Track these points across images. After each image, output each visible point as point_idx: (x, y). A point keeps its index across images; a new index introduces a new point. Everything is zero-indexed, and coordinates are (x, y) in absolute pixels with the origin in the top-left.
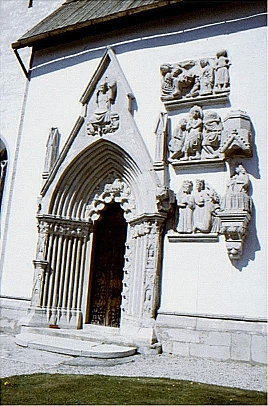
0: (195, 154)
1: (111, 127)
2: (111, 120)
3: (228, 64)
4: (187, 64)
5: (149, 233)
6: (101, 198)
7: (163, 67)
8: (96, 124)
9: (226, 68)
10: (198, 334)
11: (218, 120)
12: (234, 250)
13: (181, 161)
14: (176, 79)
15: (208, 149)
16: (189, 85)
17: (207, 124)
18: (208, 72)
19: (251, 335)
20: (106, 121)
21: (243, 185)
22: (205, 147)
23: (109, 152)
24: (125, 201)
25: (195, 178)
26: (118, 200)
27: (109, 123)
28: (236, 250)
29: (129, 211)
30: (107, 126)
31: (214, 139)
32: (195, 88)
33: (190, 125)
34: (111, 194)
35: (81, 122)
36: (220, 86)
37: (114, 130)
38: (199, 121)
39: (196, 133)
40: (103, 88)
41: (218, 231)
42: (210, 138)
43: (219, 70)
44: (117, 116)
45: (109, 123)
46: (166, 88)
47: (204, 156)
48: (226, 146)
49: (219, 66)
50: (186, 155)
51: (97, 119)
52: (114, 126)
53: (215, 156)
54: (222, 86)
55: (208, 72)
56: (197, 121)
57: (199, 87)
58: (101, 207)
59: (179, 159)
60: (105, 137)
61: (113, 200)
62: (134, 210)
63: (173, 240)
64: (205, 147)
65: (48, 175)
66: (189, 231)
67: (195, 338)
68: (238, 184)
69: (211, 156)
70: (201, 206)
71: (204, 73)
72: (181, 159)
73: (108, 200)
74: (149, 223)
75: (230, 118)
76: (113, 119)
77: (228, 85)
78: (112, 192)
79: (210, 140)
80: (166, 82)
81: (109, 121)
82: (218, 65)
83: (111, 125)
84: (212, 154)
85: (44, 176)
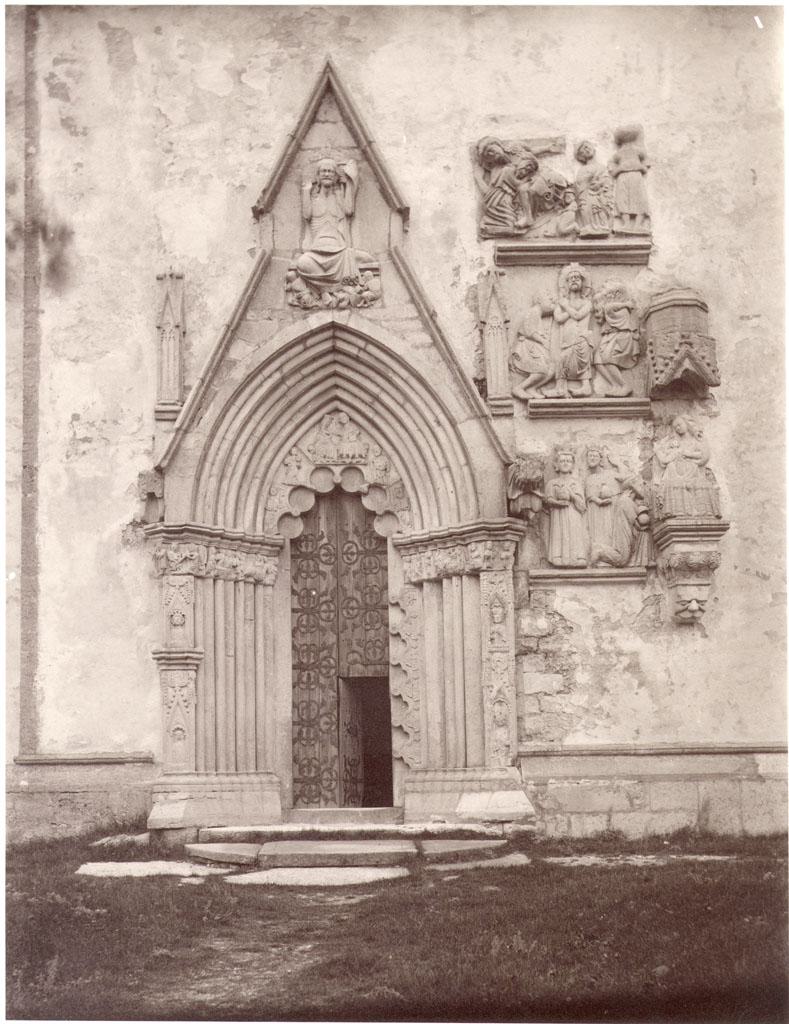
0: (577, 379)
1: (360, 292)
2: (359, 274)
4: (545, 147)
5: (489, 569)
6: (302, 478)
7: (490, 147)
9: (639, 174)
11: (629, 304)
12: (694, 602)
13: (546, 398)
14: (524, 186)
15: (610, 372)
16: (551, 200)
17: (609, 313)
18: (598, 179)
19: (740, 781)
20: (346, 274)
21: (698, 461)
22: (602, 368)
23: (340, 358)
24: (375, 486)
27: (352, 282)
28: (698, 602)
30: (346, 288)
31: (625, 350)
33: (563, 309)
34: (332, 468)
35: (265, 266)
36: (626, 218)
38: (586, 305)
39: (580, 331)
40: (327, 178)
41: (645, 563)
42: (617, 347)
43: (622, 177)
44: (375, 265)
45: (352, 282)
46: (498, 204)
47: (597, 388)
49: (622, 167)
50: (559, 383)
52: (368, 290)
53: (623, 391)
54: (633, 217)
55: (598, 179)
56: (578, 302)
60: (340, 317)
62: (407, 512)
64: (602, 368)
65: (177, 412)
66: (581, 562)
68: (687, 457)
70: (603, 505)
71: (590, 179)
72: (550, 392)
74: (489, 544)
75: (675, 306)
76: (361, 270)
77: (646, 217)
79: (620, 352)
81: (353, 277)
82: (617, 162)
83: (358, 288)
84: (621, 385)
85: (157, 412)
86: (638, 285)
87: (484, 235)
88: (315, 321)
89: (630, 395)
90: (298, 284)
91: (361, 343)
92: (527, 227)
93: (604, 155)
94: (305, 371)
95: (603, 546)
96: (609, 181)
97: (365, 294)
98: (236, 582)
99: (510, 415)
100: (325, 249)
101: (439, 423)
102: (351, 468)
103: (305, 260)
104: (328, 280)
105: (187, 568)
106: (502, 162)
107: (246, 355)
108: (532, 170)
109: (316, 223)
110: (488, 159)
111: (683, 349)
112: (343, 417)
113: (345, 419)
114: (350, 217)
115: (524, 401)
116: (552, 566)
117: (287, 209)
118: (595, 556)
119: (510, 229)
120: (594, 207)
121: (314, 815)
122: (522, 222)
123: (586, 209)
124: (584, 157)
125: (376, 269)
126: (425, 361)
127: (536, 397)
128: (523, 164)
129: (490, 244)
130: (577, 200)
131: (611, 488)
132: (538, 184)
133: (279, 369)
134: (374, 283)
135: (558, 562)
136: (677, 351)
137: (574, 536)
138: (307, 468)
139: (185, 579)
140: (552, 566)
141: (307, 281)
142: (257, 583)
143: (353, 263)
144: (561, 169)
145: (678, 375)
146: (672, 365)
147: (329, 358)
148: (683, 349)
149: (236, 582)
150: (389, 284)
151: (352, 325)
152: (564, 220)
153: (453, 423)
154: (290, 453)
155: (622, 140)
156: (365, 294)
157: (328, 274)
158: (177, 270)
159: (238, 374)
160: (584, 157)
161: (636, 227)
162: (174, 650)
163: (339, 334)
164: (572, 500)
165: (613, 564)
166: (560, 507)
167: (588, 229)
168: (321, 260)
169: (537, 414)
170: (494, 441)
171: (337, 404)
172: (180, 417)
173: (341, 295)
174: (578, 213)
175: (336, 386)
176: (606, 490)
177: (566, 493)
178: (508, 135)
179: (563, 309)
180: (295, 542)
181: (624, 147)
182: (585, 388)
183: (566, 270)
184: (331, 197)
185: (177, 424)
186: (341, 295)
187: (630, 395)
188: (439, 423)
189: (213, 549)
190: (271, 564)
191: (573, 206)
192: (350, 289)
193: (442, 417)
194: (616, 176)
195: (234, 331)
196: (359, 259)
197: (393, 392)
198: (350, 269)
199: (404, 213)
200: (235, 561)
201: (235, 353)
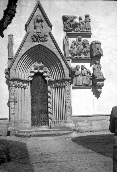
0: (80, 55)
3: (90, 21)
5: (66, 86)
6: (33, 70)
8: (38, 37)
10: (89, 122)
14: (71, 23)
16: (75, 26)
20: (42, 36)
25: (80, 64)
26: (41, 71)
29: (48, 76)
32: (78, 28)
33: (78, 43)
36: (87, 29)
37: (45, 41)
45: (43, 37)
47: (83, 56)
48: (95, 54)
51: (38, 35)
52: (46, 39)
54: (88, 29)
57: (80, 28)
58: (33, 74)
59: (74, 56)
60: (41, 43)
61: (38, 72)
63: (74, 88)
66: (82, 85)
67: (88, 124)
69: (86, 57)
73: (36, 71)
76: (45, 36)
77: (90, 29)
78: (39, 68)
80: (67, 23)
82: (86, 20)
86: (90, 40)
87: (64, 31)
88: (37, 44)
89: (88, 58)
90: (34, 37)
91: (44, 48)
92: (71, 30)
93: (84, 19)
94: (34, 52)
95: (84, 82)
96: (85, 23)
97: (45, 40)
98: (22, 88)
99: (70, 60)
100: (38, 32)
101: (57, 61)
102: (41, 68)
103: (35, 34)
104: (39, 37)
105: (14, 85)
106: (67, 19)
107: (24, 50)
108: (72, 21)
109: (37, 27)
110: (65, 19)
111: (98, 51)
112: (40, 60)
113: (40, 61)
114: (42, 27)
115: (72, 58)
116: (76, 85)
117: (31, 24)
118: (84, 84)
119: (69, 30)
120: (82, 27)
121: (35, 128)
122: (71, 29)
123: (81, 27)
124: (80, 19)
125: (47, 36)
126: (55, 50)
127: (74, 58)
128: (71, 20)
129: (65, 33)
130: (80, 26)
131: (86, 73)
132: (73, 23)
133: (30, 52)
134: (47, 38)
135: (78, 85)
136: (97, 51)
137: (80, 80)
138: (33, 68)
139: (13, 87)
140: (76, 85)
141: (35, 37)
142: (25, 88)
143: (43, 35)
144: (77, 20)
145: (97, 55)
146: (96, 53)
147: (38, 50)
148: (98, 51)
149: (22, 88)
150: (49, 38)
151: (43, 45)
152: (78, 29)
153: (60, 62)
154: (30, 66)
155: (87, 16)
156: (45, 40)
157: (39, 36)
158: (12, 34)
159: (23, 52)
160: (80, 19)
161: (88, 30)
162: (12, 99)
163: (40, 46)
164: (80, 74)
165: (86, 85)
166: (78, 76)
167: (81, 30)
168: (38, 34)
169: (74, 61)
170: (67, 65)
171: (39, 58)
172: (13, 60)
173: (41, 40)
174: (80, 28)
175: (39, 55)
176: (85, 73)
177: (79, 73)
178: (68, 14)
179: (78, 43)
180: (31, 81)
181: (87, 18)
182: (82, 56)
183: (78, 37)
184: (39, 23)
185: (12, 61)
186: (41, 40)
187: (88, 58)
188: (57, 61)
189: (18, 82)
190: (27, 85)
191: (79, 27)
192: (43, 39)
193: (58, 61)
194: (86, 22)
195: (22, 45)
196: (44, 34)
197: (49, 56)
198: (43, 36)
199: (51, 26)
200: (22, 84)
201: (23, 48)
